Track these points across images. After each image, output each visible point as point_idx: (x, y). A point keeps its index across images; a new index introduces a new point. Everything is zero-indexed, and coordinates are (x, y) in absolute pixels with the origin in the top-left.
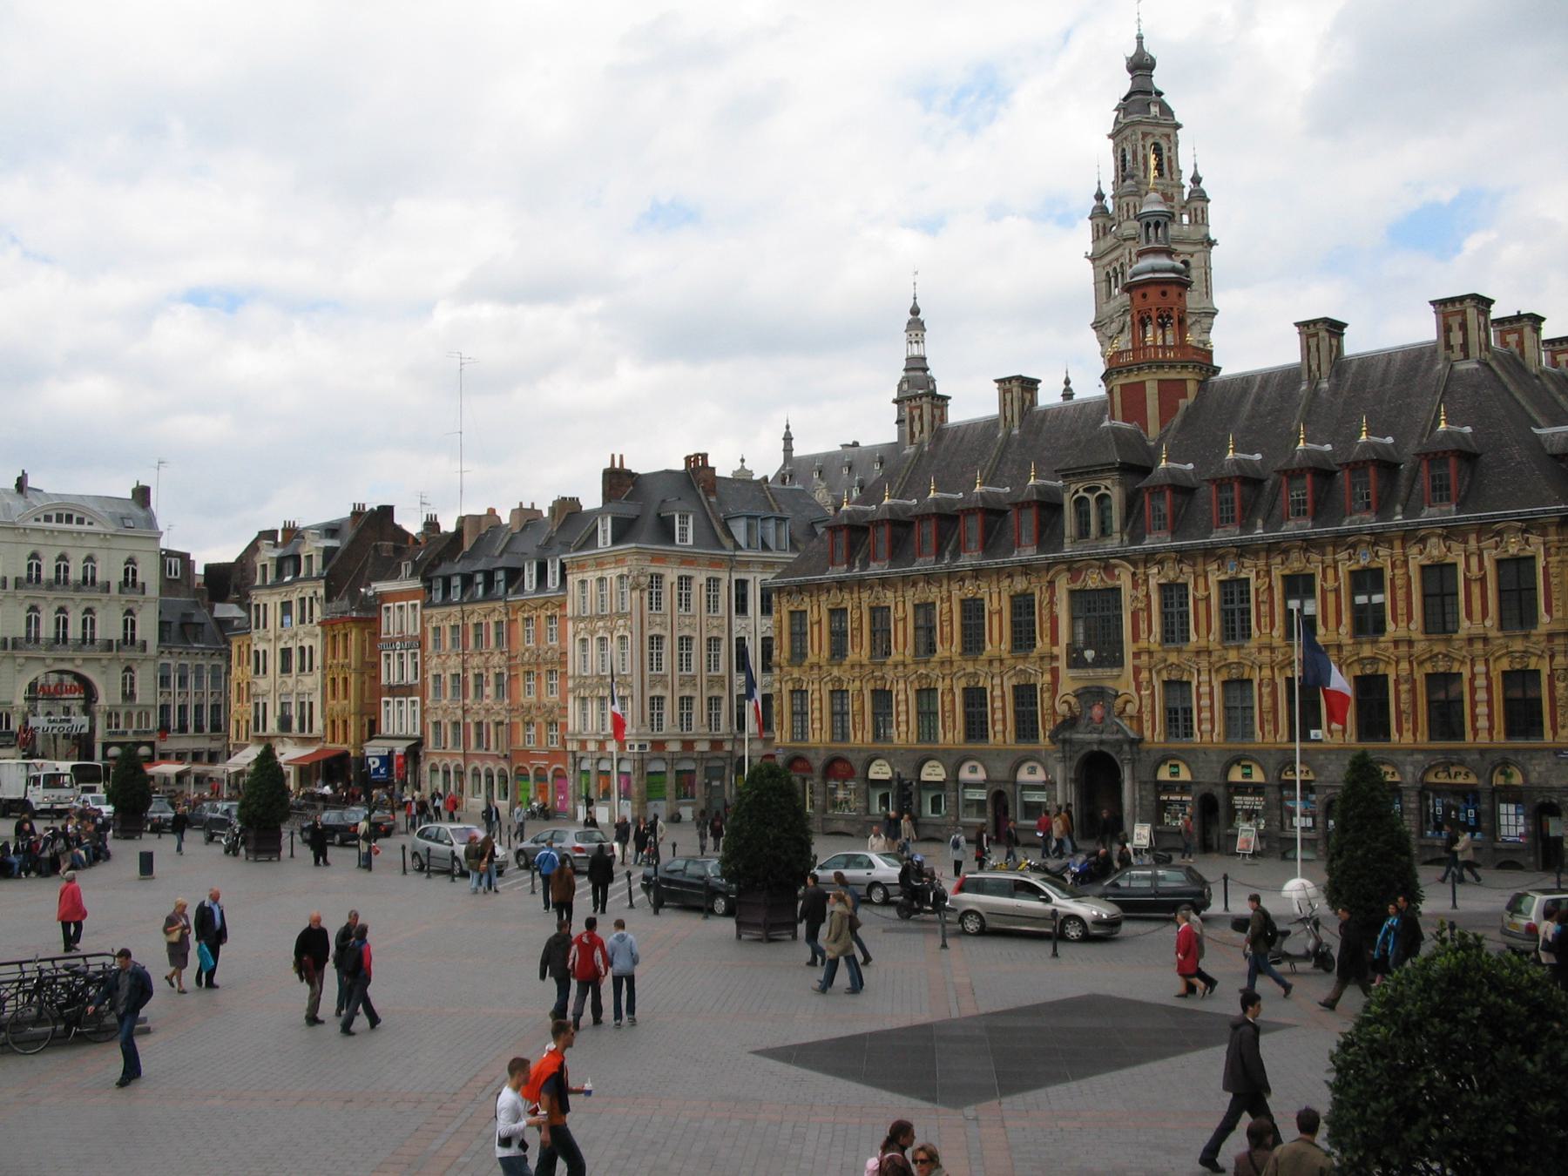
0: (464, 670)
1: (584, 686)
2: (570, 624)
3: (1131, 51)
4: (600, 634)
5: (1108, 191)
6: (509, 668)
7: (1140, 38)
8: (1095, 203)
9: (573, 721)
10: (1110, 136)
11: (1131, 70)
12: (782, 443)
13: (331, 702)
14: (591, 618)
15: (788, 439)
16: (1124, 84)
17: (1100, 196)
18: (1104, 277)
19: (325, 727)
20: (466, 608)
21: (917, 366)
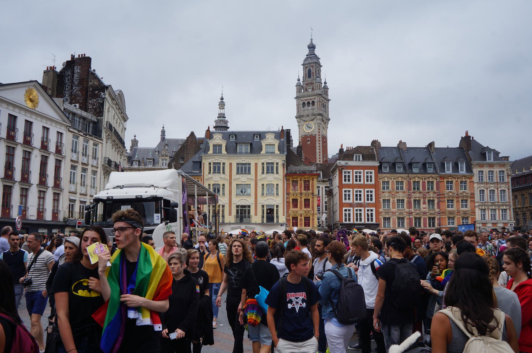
0: (409, 198)
1: (485, 206)
2: (476, 185)
3: (309, 43)
4: (492, 189)
5: (301, 80)
6: (438, 198)
7: (311, 39)
8: (297, 82)
9: (478, 217)
10: (302, 65)
11: (309, 47)
12: (160, 133)
13: (292, 209)
14: (487, 183)
15: (163, 132)
16: (307, 51)
17: (299, 80)
18: (301, 103)
19: (288, 220)
20: (410, 175)
21: (222, 116)
